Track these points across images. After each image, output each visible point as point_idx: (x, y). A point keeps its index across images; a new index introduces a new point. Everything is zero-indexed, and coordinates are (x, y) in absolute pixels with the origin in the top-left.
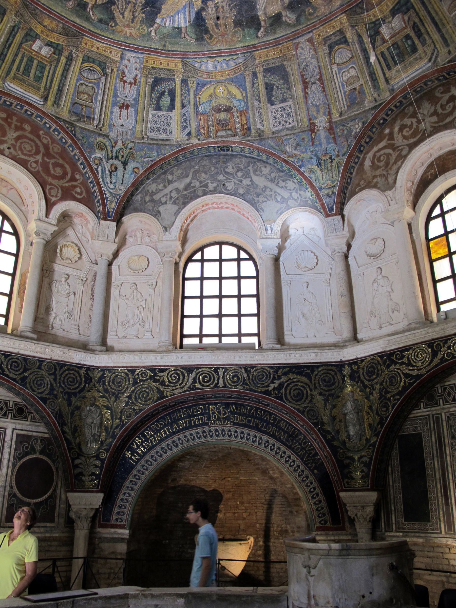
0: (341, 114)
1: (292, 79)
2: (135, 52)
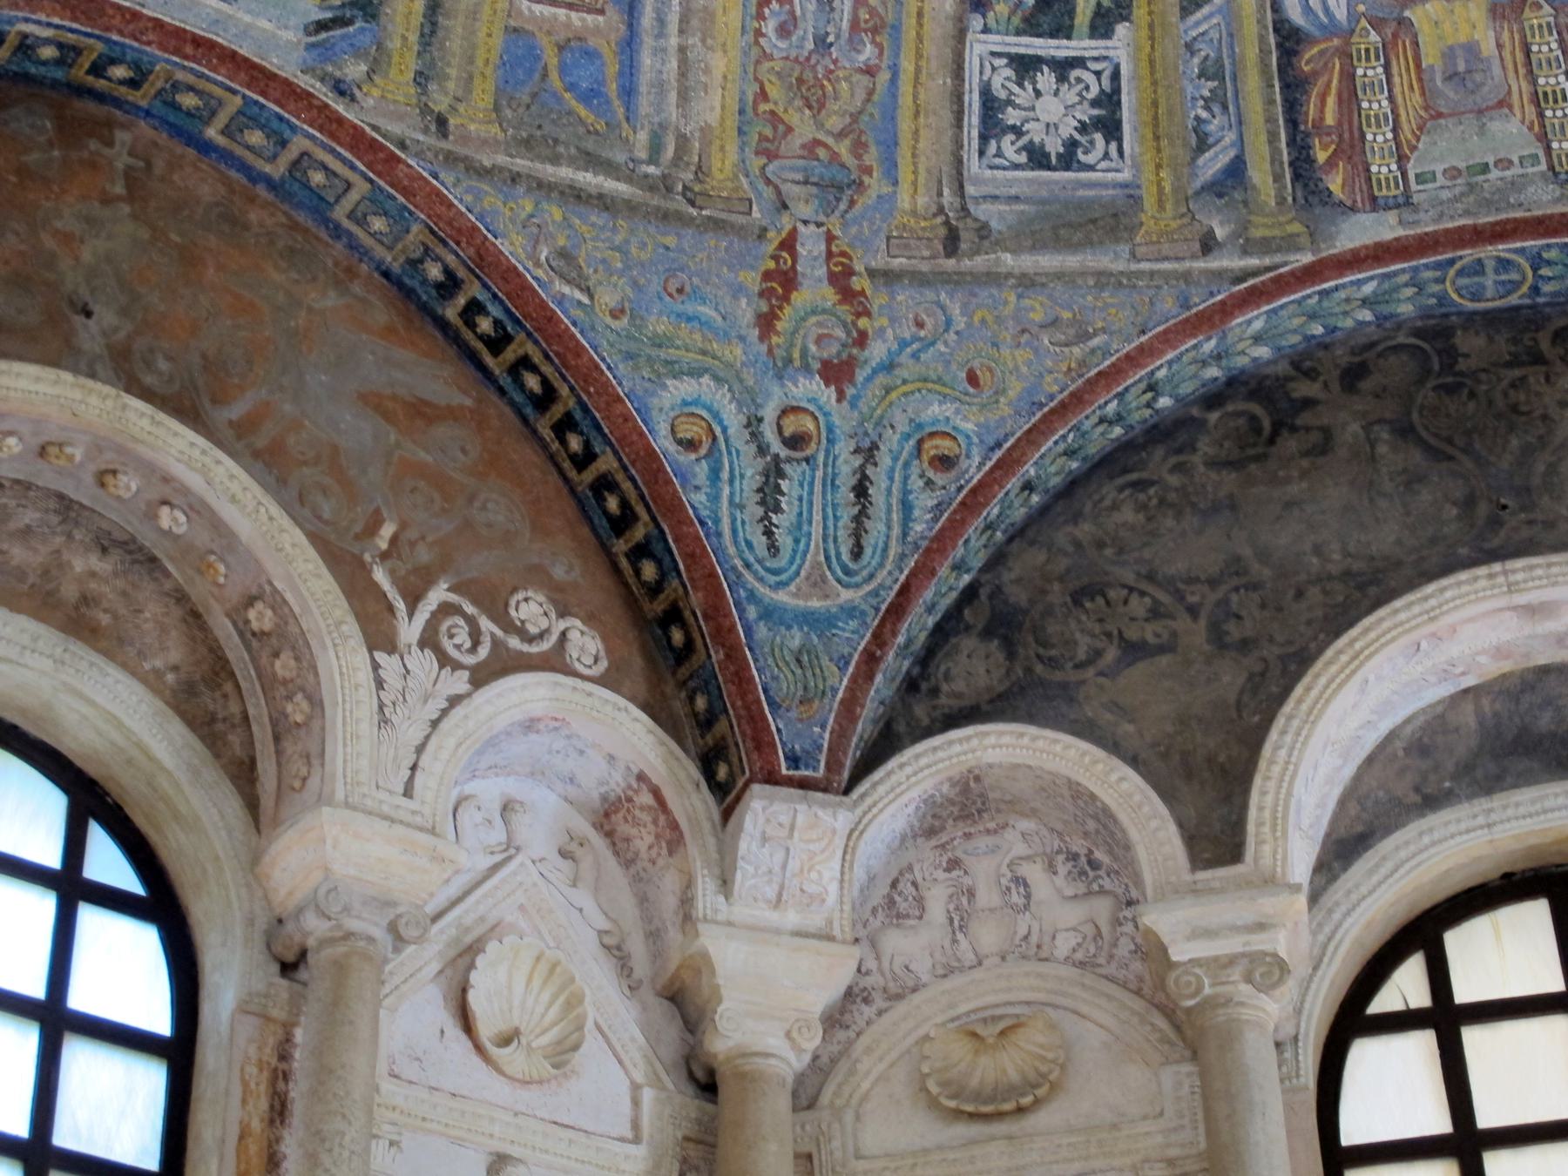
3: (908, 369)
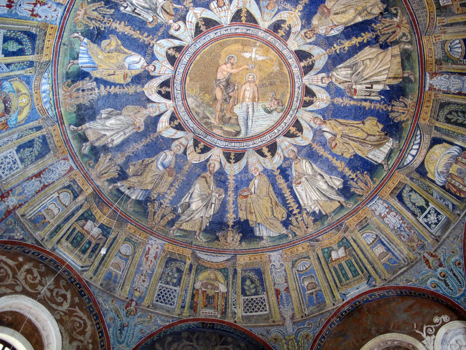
0: (23, 216)
1: (40, 162)
2: (62, 17)
3: (446, 258)
